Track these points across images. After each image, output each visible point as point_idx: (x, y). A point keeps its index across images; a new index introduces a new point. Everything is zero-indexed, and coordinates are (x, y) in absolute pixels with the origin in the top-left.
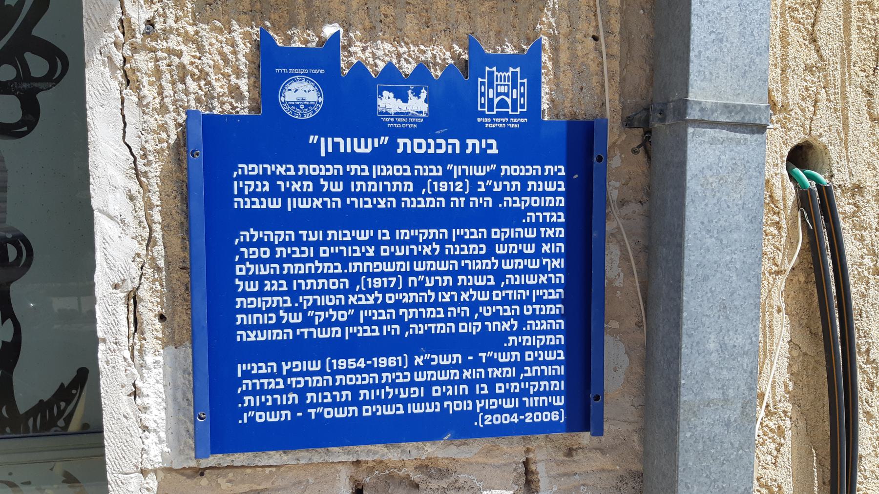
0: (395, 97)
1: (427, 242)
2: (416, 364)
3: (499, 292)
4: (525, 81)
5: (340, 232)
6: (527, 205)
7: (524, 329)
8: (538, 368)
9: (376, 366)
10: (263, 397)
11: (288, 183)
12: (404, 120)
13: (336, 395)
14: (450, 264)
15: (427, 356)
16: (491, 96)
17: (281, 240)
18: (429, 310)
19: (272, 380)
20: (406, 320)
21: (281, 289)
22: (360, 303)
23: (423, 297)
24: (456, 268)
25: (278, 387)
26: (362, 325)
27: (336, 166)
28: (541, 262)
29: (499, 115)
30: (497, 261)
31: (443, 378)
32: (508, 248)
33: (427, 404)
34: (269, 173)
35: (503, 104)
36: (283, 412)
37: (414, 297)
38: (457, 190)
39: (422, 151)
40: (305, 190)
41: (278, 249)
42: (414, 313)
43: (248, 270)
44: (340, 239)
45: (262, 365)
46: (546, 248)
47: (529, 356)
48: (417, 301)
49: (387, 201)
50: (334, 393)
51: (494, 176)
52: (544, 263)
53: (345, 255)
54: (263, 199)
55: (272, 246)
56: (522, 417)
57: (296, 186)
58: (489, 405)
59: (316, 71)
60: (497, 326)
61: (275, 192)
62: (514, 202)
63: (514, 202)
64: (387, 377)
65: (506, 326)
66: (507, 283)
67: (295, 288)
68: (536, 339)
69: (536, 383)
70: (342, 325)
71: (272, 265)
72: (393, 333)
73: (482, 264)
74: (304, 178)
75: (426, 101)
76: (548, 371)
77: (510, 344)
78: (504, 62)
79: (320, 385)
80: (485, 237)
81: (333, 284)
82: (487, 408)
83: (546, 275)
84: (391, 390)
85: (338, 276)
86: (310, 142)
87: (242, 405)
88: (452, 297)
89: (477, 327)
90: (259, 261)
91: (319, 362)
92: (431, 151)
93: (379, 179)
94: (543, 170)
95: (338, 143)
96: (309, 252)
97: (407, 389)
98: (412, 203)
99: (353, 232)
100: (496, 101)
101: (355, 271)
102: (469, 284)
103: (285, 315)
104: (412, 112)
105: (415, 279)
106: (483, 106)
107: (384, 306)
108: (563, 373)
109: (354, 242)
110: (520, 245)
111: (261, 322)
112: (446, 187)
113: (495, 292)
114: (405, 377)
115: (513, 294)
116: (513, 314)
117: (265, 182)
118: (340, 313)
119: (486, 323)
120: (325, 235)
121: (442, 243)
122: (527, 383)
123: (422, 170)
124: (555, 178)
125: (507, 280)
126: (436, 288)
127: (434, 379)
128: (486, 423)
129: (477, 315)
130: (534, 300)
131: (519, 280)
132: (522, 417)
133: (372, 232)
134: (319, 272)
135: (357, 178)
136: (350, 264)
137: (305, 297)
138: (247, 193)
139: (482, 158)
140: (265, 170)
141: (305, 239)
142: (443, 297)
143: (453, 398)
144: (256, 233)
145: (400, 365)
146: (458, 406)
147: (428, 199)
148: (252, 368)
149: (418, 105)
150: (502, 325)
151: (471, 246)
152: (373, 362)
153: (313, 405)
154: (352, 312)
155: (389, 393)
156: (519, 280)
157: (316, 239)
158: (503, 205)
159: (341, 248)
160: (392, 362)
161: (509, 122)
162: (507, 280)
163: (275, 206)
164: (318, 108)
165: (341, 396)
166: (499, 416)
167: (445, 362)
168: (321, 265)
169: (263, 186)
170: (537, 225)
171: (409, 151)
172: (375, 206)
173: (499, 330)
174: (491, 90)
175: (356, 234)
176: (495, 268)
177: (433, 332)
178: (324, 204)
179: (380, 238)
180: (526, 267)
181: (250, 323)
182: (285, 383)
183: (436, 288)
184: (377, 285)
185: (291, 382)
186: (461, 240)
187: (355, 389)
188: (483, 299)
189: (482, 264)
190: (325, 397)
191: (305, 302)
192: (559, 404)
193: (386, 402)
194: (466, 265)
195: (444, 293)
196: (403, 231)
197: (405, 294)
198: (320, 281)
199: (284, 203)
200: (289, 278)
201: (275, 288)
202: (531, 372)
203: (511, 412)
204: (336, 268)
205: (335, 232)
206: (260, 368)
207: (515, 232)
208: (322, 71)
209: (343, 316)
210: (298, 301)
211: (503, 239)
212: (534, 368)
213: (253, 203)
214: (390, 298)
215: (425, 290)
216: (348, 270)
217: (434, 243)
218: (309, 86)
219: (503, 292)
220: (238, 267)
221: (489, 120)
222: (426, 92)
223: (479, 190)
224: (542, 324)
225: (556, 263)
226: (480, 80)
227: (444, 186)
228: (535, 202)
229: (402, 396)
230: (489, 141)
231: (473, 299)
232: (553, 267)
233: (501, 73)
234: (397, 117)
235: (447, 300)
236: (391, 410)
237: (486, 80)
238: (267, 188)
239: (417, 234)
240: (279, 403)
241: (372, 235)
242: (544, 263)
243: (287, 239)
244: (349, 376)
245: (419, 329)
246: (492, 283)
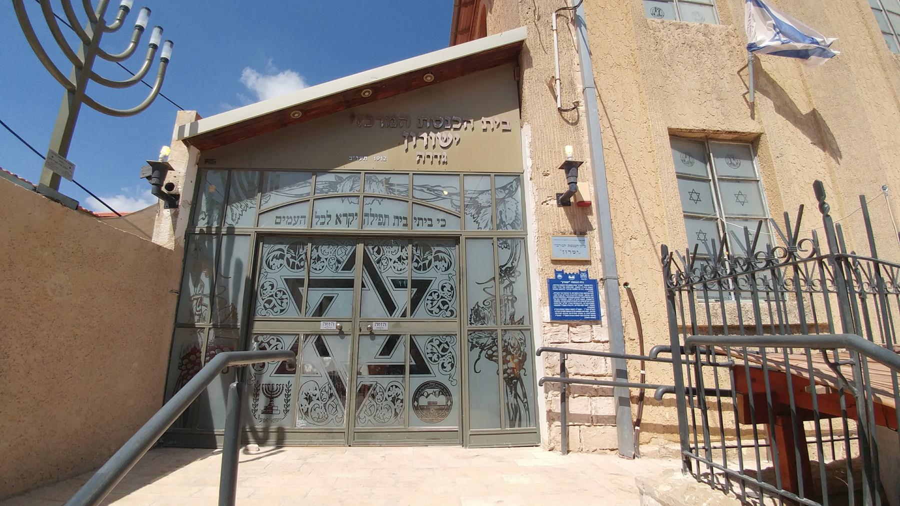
78: (583, 272)
123: (574, 285)
139: (582, 284)
149: (573, 277)
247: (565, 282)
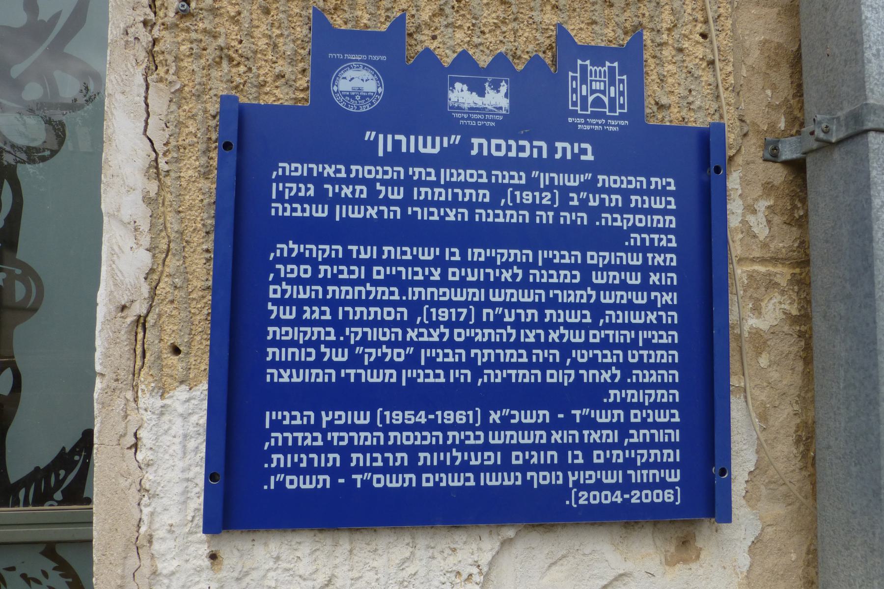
0: (469, 90)
1: (507, 265)
4: (625, 77)
5: (399, 249)
6: (630, 224)
7: (629, 380)
8: (646, 431)
9: (440, 421)
10: (296, 456)
11: (337, 187)
12: (479, 116)
13: (388, 458)
14: (535, 294)
15: (506, 412)
16: (584, 93)
17: (326, 256)
18: (508, 352)
19: (308, 434)
20: (479, 363)
21: (323, 318)
22: (421, 339)
23: (501, 335)
24: (543, 300)
25: (315, 444)
26: (423, 368)
27: (396, 169)
29: (594, 115)
30: (594, 293)
31: (526, 441)
32: (608, 276)
33: (505, 474)
34: (315, 174)
35: (598, 102)
36: (321, 477)
37: (490, 334)
38: (544, 202)
39: (502, 154)
40: (357, 196)
42: (489, 355)
43: (284, 292)
44: (398, 257)
45: (297, 413)
46: (654, 278)
47: (636, 416)
48: (493, 340)
49: (457, 213)
50: (386, 455)
51: (590, 187)
52: (653, 298)
53: (404, 277)
54: (306, 206)
55: (314, 263)
56: (627, 496)
57: (347, 191)
58: (585, 479)
59: (376, 58)
60: (594, 375)
61: (320, 198)
62: (614, 220)
63: (614, 220)
64: (454, 437)
65: (606, 376)
66: (607, 321)
67: (340, 317)
68: (644, 394)
69: (645, 452)
70: (398, 367)
71: (314, 287)
72: (462, 380)
73: (576, 295)
74: (357, 181)
75: (506, 96)
76: (660, 436)
77: (611, 400)
78: (598, 54)
79: (368, 443)
80: (579, 261)
81: (389, 314)
82: (582, 482)
83: (655, 313)
84: (459, 454)
85: (395, 304)
86: (366, 139)
87: (269, 465)
88: (537, 336)
89: (569, 376)
90: (298, 281)
91: (368, 413)
92: (513, 154)
93: (448, 185)
94: (649, 183)
95: (400, 141)
96: (359, 272)
97: (479, 454)
98: (488, 216)
99: (415, 249)
100: (590, 99)
101: (415, 298)
102: (559, 321)
103: (328, 350)
104: (490, 108)
105: (490, 311)
106: (575, 104)
107: (452, 344)
108: (678, 440)
109: (416, 261)
110: (623, 274)
111: (297, 359)
112: (530, 197)
113: (591, 332)
114: (477, 438)
115: (614, 335)
116: (615, 361)
117: (309, 186)
118: (396, 351)
119: (581, 372)
120: (380, 252)
121: (526, 267)
122: (633, 452)
123: (501, 176)
124: (664, 192)
125: (607, 318)
126: (518, 324)
127: (514, 441)
128: (581, 502)
129: (569, 361)
130: (641, 344)
131: (622, 317)
132: (627, 496)
133: (438, 250)
134: (371, 297)
135: (421, 183)
136: (410, 289)
137: (353, 329)
138: (287, 197)
139: (574, 165)
140: (310, 170)
141: (355, 256)
142: (526, 336)
143: (538, 468)
144: (296, 247)
145: (471, 421)
146: (544, 478)
147: (508, 212)
148: (284, 417)
150: (601, 374)
151: (562, 273)
152: (436, 416)
153: (359, 470)
155: (456, 458)
156: (622, 317)
157: (368, 256)
158: (601, 223)
159: (399, 269)
160: (460, 417)
161: (606, 124)
162: (607, 318)
163: (320, 215)
164: (377, 100)
165: (395, 459)
166: (597, 493)
167: (528, 421)
168: (373, 289)
169: (307, 189)
170: (643, 249)
171: (485, 153)
172: (442, 218)
173: (597, 380)
174: (584, 87)
175: (418, 251)
176: (592, 301)
177: (514, 380)
178: (380, 213)
179: (447, 258)
180: (630, 301)
181: (283, 359)
182: (324, 438)
183: (518, 324)
184: (443, 317)
185: (332, 437)
186: (549, 264)
187: (413, 451)
188: (577, 340)
189: (576, 295)
190: (374, 460)
191: (353, 335)
192: (673, 480)
193: (452, 469)
194: (556, 296)
195: (528, 331)
196: (476, 251)
197: (478, 331)
198: (372, 310)
199: (332, 212)
200: (334, 304)
201: (316, 315)
202: (638, 437)
203: (612, 488)
204: (392, 293)
205: (392, 249)
206: (293, 418)
207: (616, 257)
208: (384, 58)
209: (399, 355)
210: (343, 334)
211: (601, 266)
212: (642, 432)
213: (294, 210)
214: (459, 335)
215: (504, 326)
216: (407, 297)
217: (515, 267)
218: (365, 74)
219: (602, 332)
220: (272, 287)
221: (583, 121)
222: (506, 86)
223: (571, 203)
224: (651, 375)
225: (667, 298)
226: (571, 74)
227: (528, 197)
228: (640, 221)
230: (583, 146)
231: (565, 340)
232: (664, 302)
233: (595, 67)
234: (471, 113)
235: (532, 339)
237: (578, 75)
238: (311, 193)
239: (493, 255)
240: (316, 465)
241: (438, 253)
242: (653, 298)
243: (333, 256)
244: (405, 434)
245: (496, 376)
246: (588, 320)
247: (409, 143)
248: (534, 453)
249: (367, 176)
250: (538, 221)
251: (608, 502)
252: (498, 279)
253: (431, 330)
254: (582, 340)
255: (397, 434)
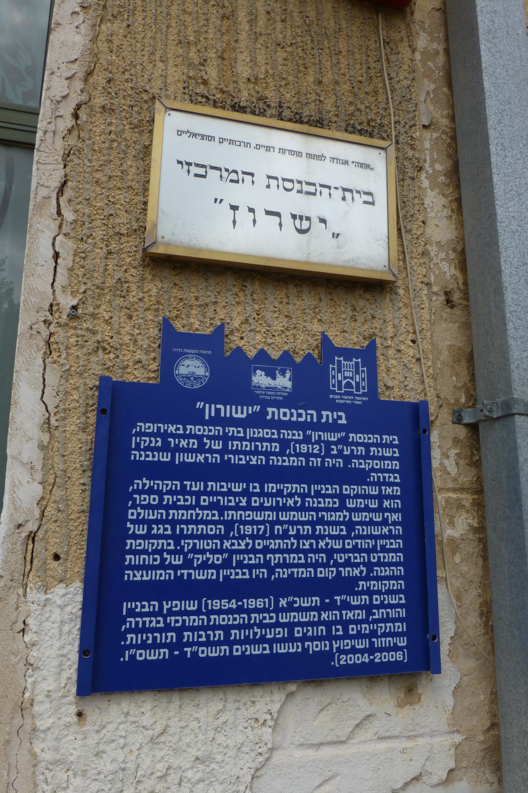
0: (266, 375)
2: (281, 606)
3: (350, 541)
5: (218, 483)
6: (370, 467)
7: (372, 575)
8: (383, 610)
9: (245, 607)
11: (177, 440)
12: (272, 393)
13: (210, 635)
16: (340, 379)
17: (168, 488)
18: (292, 556)
20: (273, 564)
21: (166, 533)
22: (233, 548)
23: (287, 544)
24: (315, 519)
26: (235, 568)
27: (217, 428)
28: (383, 516)
30: (348, 514)
31: (304, 620)
32: (357, 502)
34: (162, 431)
37: (279, 544)
38: (315, 451)
40: (190, 446)
41: (166, 497)
42: (279, 558)
43: (139, 514)
44: (218, 490)
45: (145, 603)
48: (282, 547)
49: (258, 459)
51: (344, 441)
53: (222, 504)
54: (155, 453)
56: (372, 657)
58: (344, 646)
60: (349, 571)
62: (360, 464)
63: (360, 464)
64: (255, 618)
67: (178, 533)
69: (383, 625)
72: (261, 577)
73: (336, 516)
75: (290, 380)
77: (360, 589)
80: (338, 492)
82: (342, 648)
89: (332, 572)
91: (196, 602)
95: (220, 409)
97: (273, 630)
99: (229, 484)
101: (230, 518)
104: (279, 387)
105: (280, 527)
111: (147, 563)
112: (306, 448)
113: (347, 541)
114: (271, 618)
115: (361, 543)
116: (362, 561)
117: (158, 439)
118: (216, 556)
119: (340, 569)
120: (206, 486)
122: (375, 625)
127: (296, 620)
128: (342, 663)
129: (332, 561)
130: (379, 549)
132: (372, 657)
133: (245, 484)
134: (199, 518)
135: (233, 438)
136: (226, 512)
137: (186, 541)
141: (188, 489)
142: (304, 544)
144: (148, 482)
145: (267, 606)
146: (317, 646)
150: (353, 570)
151: (327, 500)
152: (243, 603)
153: (189, 644)
154: (226, 555)
155: (257, 633)
159: (219, 498)
161: (354, 400)
163: (165, 459)
166: (352, 656)
167: (306, 605)
168: (201, 512)
169: (157, 442)
173: (351, 575)
174: (340, 374)
176: (347, 519)
177: (295, 576)
179: (251, 490)
181: (137, 563)
182: (165, 621)
188: (337, 547)
189: (336, 516)
191: (186, 545)
194: (323, 516)
195: (304, 541)
197: (272, 541)
198: (200, 527)
202: (379, 615)
204: (213, 515)
205: (214, 484)
207: (362, 489)
209: (218, 559)
210: (179, 544)
214: (259, 544)
215: (289, 537)
217: (296, 497)
221: (339, 397)
223: (332, 452)
224: (386, 571)
226: (331, 366)
229: (268, 636)
230: (340, 414)
231: (329, 547)
235: (307, 547)
236: (259, 650)
239: (282, 488)
240: (158, 641)
241: (245, 487)
243: (174, 488)
248: (309, 628)
249: (198, 433)
250: (311, 465)
251: (360, 662)
252: (285, 505)
253: (240, 541)
254: (341, 547)
255: (216, 617)
